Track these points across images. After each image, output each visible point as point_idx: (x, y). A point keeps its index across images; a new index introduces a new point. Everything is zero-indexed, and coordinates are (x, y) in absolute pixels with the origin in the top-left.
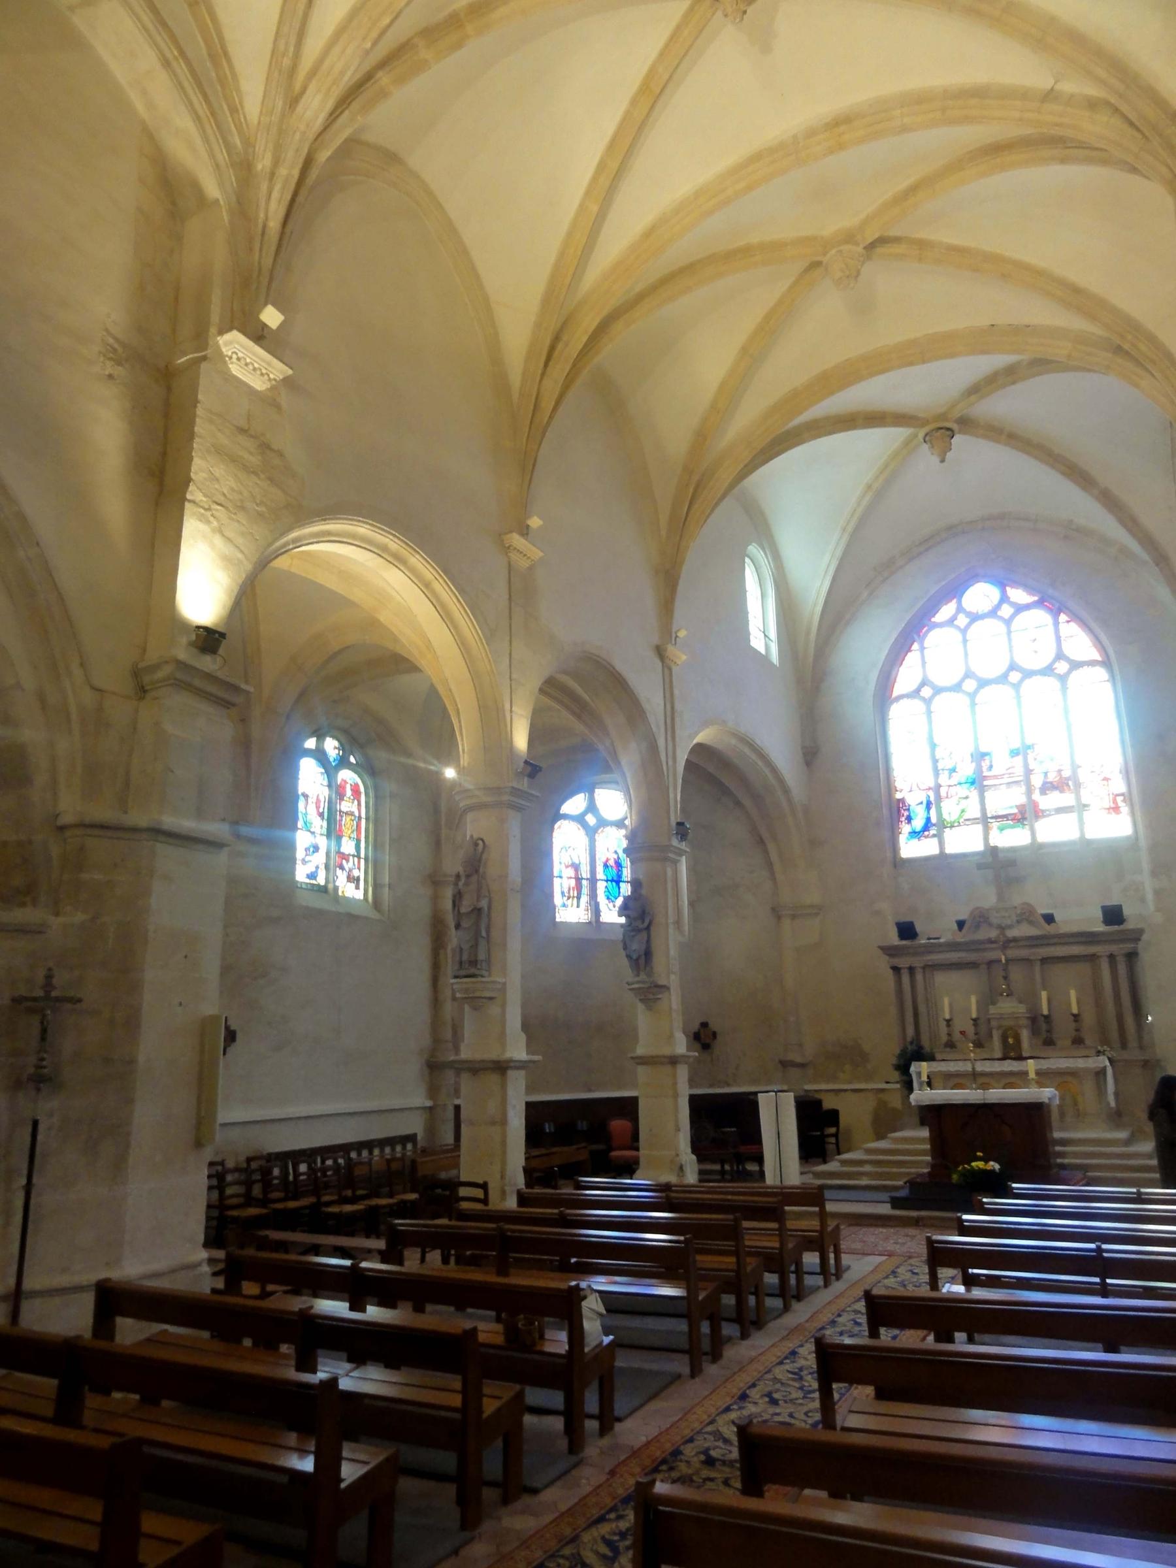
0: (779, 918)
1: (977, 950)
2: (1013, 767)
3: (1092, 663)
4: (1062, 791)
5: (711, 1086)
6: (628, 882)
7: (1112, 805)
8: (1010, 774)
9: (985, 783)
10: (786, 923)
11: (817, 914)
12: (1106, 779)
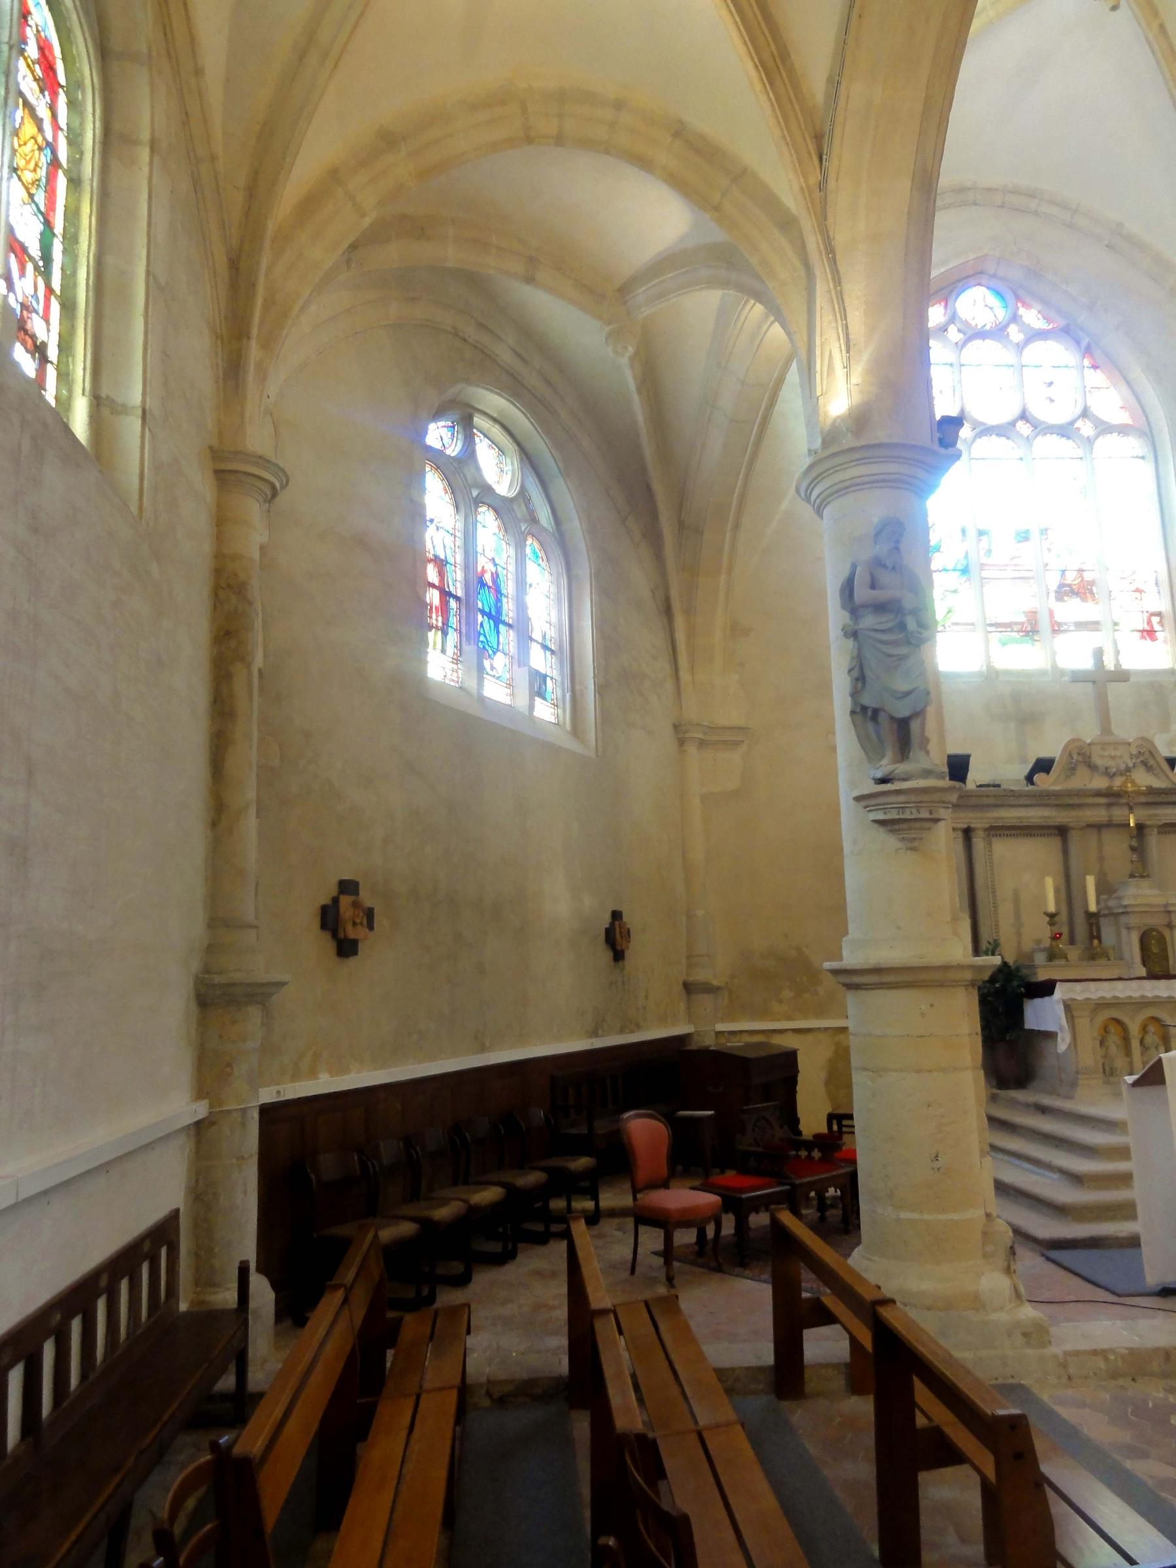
0: (681, 742)
1: (1073, 806)
2: (1019, 557)
3: (1123, 430)
4: (1084, 600)
5: (622, 1031)
6: (510, 626)
7: (1147, 628)
8: (1016, 565)
9: (984, 574)
10: (692, 749)
11: (737, 744)
12: (1138, 590)
